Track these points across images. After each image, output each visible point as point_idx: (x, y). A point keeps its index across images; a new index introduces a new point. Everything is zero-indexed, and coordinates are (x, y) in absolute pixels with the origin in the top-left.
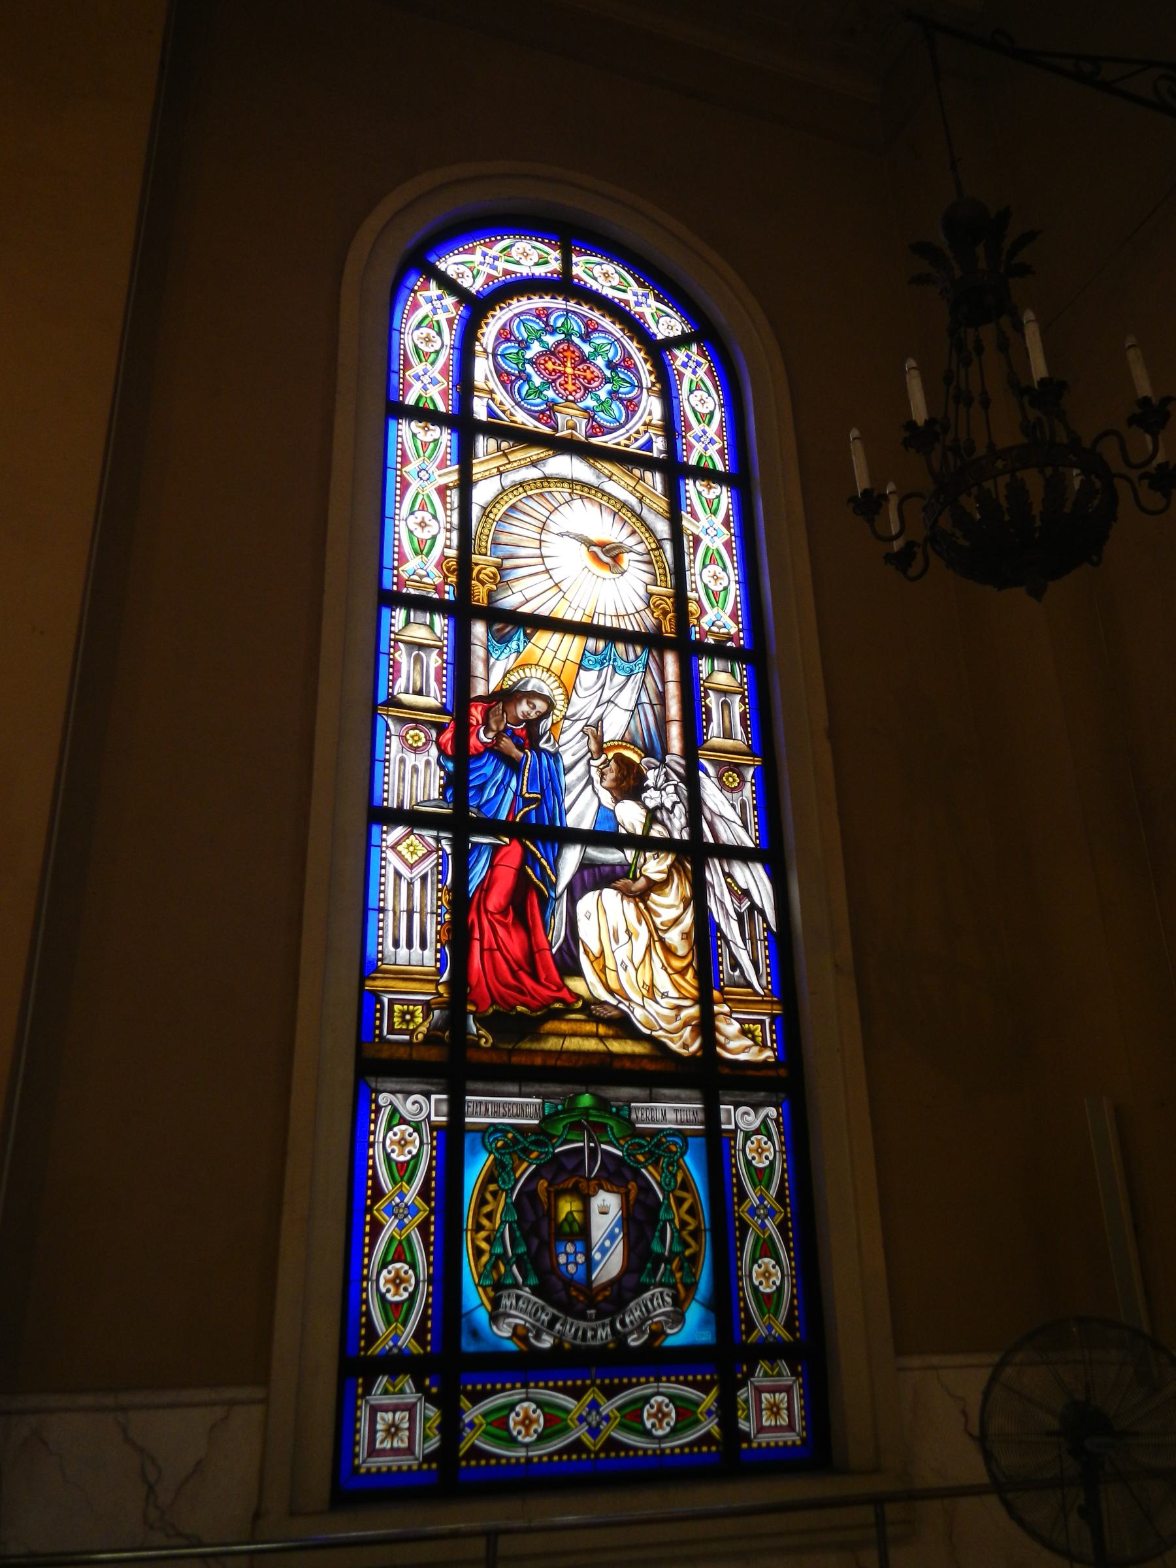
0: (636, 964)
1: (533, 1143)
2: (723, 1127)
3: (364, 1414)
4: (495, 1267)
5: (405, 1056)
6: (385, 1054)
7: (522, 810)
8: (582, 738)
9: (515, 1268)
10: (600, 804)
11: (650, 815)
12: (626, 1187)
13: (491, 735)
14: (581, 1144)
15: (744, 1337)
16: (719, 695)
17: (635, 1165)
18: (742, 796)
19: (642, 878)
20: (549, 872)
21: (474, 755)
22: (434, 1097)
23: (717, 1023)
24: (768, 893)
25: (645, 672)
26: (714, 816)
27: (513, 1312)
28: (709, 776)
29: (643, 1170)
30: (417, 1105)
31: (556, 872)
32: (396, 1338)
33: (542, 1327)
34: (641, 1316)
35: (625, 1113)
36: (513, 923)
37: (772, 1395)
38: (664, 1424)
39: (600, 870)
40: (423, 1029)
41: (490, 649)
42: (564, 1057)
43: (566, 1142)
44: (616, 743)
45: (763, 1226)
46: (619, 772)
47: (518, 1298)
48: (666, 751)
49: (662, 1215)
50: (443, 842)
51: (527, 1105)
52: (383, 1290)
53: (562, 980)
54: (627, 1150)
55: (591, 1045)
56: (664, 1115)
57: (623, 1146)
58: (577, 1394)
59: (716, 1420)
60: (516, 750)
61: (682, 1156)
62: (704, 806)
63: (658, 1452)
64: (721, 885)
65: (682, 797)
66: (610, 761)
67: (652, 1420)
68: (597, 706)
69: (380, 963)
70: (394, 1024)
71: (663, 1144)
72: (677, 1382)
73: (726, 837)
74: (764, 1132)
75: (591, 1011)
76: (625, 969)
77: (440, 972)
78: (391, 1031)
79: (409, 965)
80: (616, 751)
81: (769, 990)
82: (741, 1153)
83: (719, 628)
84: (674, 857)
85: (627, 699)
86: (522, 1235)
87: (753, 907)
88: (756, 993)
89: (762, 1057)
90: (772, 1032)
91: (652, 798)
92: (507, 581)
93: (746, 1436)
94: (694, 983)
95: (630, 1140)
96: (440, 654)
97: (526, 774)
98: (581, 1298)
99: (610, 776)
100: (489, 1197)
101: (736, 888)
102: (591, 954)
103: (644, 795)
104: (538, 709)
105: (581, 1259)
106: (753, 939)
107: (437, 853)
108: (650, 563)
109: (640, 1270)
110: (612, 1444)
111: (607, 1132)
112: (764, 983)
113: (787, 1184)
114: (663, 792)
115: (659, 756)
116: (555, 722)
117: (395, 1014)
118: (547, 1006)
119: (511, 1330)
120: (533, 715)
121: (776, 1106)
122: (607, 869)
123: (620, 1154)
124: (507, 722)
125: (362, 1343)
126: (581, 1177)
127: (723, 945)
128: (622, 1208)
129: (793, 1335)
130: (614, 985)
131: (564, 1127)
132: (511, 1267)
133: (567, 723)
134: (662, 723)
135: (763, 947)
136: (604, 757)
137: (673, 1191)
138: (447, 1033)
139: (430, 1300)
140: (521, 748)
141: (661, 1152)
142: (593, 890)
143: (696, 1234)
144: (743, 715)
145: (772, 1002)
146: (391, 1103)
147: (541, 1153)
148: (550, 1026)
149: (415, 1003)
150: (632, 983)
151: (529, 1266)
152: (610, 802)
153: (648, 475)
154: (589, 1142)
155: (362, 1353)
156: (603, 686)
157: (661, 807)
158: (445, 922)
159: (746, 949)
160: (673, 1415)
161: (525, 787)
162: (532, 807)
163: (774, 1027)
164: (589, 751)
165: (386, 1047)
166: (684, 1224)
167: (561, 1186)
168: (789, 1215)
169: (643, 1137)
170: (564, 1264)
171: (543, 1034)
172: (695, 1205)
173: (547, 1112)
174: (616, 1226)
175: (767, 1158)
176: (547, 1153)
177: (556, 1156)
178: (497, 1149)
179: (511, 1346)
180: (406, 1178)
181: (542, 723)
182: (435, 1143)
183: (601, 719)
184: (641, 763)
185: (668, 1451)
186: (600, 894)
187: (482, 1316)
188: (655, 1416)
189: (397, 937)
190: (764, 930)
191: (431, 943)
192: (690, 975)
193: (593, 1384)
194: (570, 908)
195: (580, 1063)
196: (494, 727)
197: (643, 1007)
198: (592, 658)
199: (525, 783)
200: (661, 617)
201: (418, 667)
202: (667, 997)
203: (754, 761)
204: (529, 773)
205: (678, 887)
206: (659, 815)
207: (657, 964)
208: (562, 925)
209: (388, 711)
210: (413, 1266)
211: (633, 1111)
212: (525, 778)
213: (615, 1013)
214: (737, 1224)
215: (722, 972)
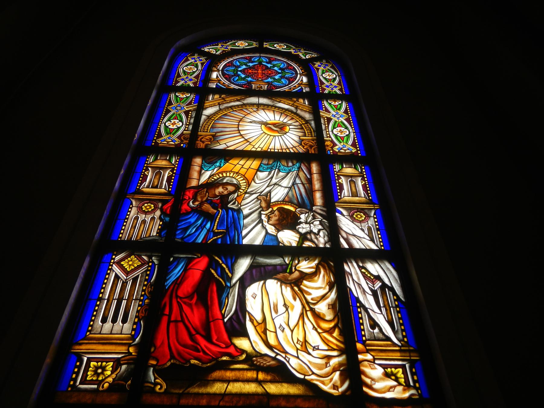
0: (292, 324)
6: (74, 400)
7: (212, 238)
8: (257, 201)
10: (267, 233)
11: (302, 237)
13: (197, 203)
16: (347, 178)
18: (368, 224)
19: (297, 273)
20: (227, 271)
21: (183, 213)
23: (362, 368)
24: (394, 277)
25: (299, 171)
26: (348, 235)
28: (344, 216)
31: (232, 271)
36: (196, 303)
39: (265, 269)
40: (110, 380)
41: (203, 167)
42: (226, 399)
44: (279, 203)
46: (281, 216)
48: (313, 204)
50: (153, 258)
53: (231, 340)
55: (251, 388)
60: (212, 210)
62: (341, 230)
64: (357, 274)
65: (325, 227)
66: (275, 211)
68: (268, 186)
73: (357, 245)
76: (283, 331)
77: (133, 338)
79: (111, 334)
80: (279, 206)
83: (345, 150)
84: (320, 259)
85: (287, 182)
87: (384, 286)
88: (395, 345)
89: (406, 395)
90: (413, 374)
91: (303, 228)
92: (217, 141)
96: (172, 171)
97: (217, 220)
99: (274, 219)
101: (369, 275)
102: (255, 321)
103: (297, 227)
104: (229, 190)
106: (387, 308)
107: (148, 264)
108: (302, 128)
112: (400, 336)
114: (311, 225)
115: (309, 207)
116: (239, 195)
118: (216, 359)
120: (226, 192)
122: (270, 268)
124: (208, 197)
127: (363, 312)
130: (272, 341)
133: (247, 195)
134: (310, 192)
135: (396, 311)
136: (270, 209)
140: (214, 207)
142: (259, 280)
144: (364, 187)
145: (409, 351)
148: (217, 374)
149: (107, 360)
150: (289, 341)
152: (274, 231)
153: (301, 101)
156: (272, 178)
157: (311, 232)
158: (145, 305)
159: (382, 313)
161: (215, 227)
162: (219, 236)
163: (414, 370)
164: (261, 207)
171: (211, 380)
181: (231, 196)
183: (270, 192)
184: (296, 211)
186: (265, 283)
190: (395, 300)
191: (131, 318)
192: (336, 334)
194: (241, 292)
195: (241, 403)
196: (199, 199)
197: (298, 357)
198: (266, 167)
199: (216, 224)
200: (309, 148)
201: (158, 177)
202: (318, 349)
203: (374, 206)
204: (219, 220)
205: (324, 276)
206: (309, 236)
207: (309, 326)
208: (233, 303)
209: (134, 196)
212: (216, 222)
213: (273, 362)
215: (364, 330)
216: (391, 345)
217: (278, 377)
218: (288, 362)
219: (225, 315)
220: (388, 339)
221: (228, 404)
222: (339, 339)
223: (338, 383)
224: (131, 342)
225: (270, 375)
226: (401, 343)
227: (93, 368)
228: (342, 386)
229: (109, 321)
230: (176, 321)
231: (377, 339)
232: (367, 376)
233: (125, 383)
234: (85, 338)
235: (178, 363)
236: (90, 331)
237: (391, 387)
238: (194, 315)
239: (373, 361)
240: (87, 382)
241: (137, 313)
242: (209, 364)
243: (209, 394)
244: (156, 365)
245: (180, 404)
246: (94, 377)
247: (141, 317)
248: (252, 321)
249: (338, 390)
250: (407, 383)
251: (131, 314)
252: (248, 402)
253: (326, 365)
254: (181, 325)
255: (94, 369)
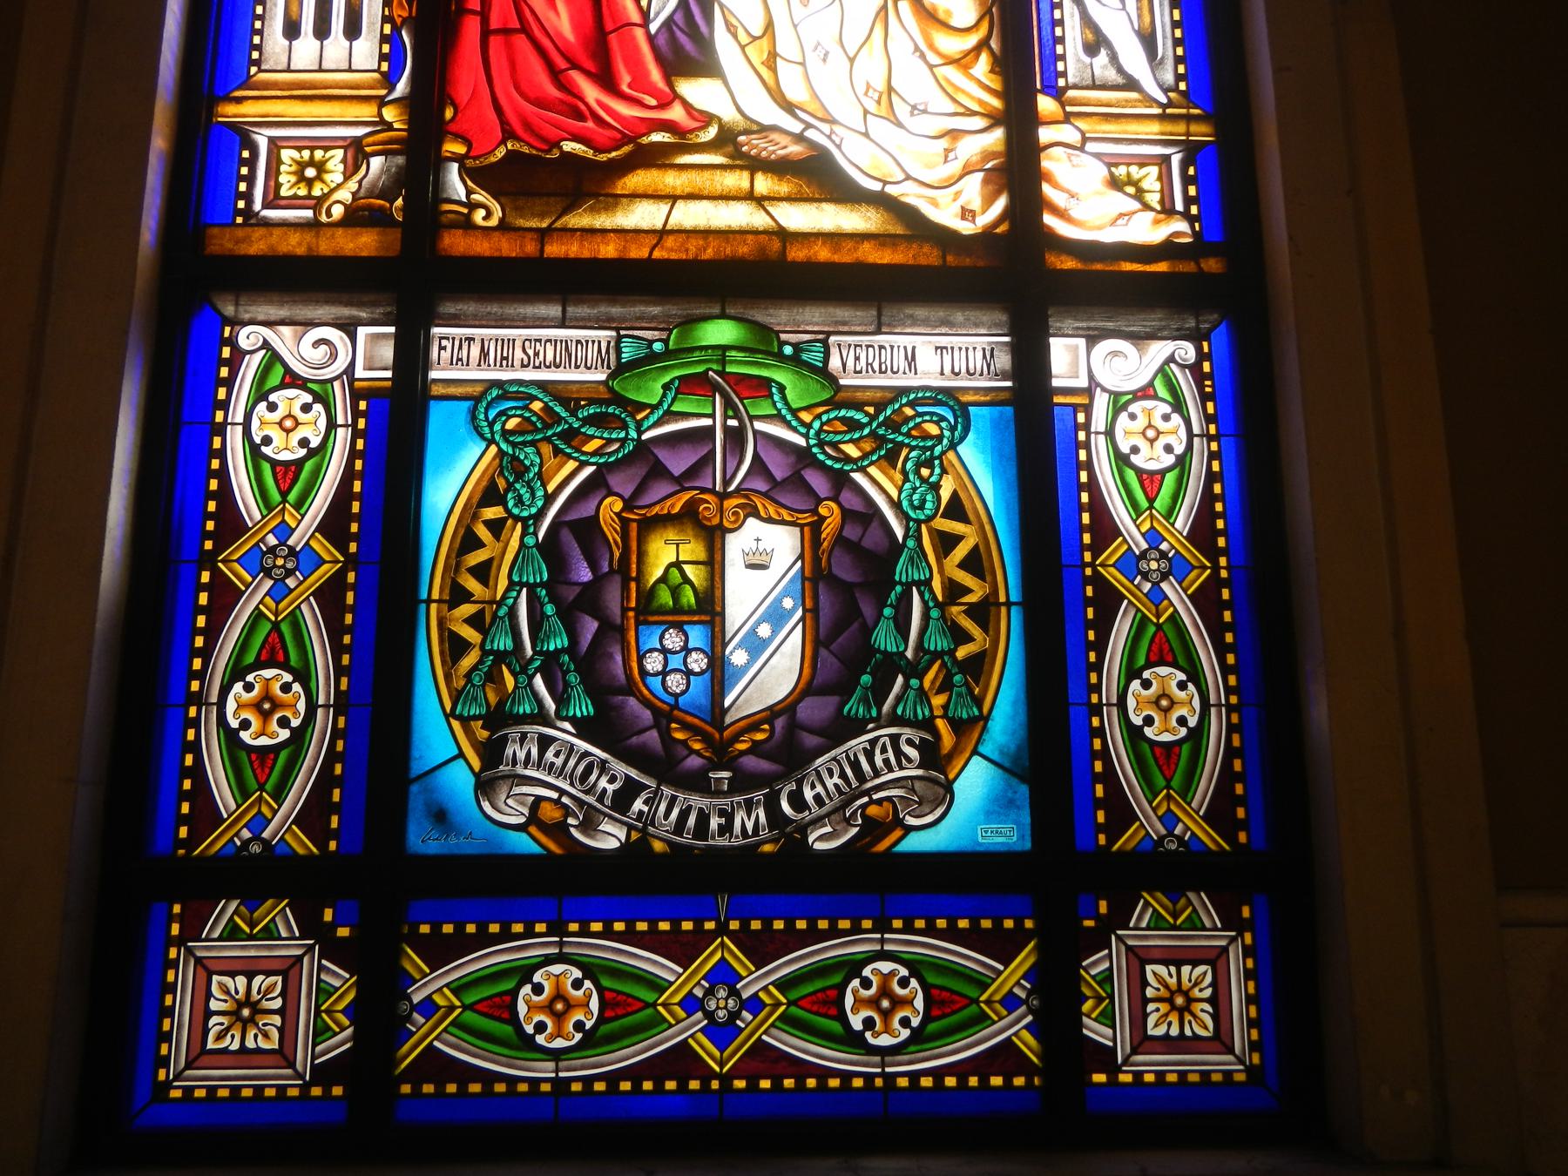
1: (589, 421)
2: (1056, 383)
3: (183, 977)
4: (493, 677)
5: (301, 251)
6: (258, 244)
9: (539, 682)
12: (815, 512)
14: (708, 422)
15: (1102, 839)
17: (837, 466)
22: (362, 332)
23: (1046, 164)
27: (528, 772)
29: (858, 477)
30: (324, 348)
32: (260, 822)
33: (599, 806)
34: (846, 789)
35: (814, 356)
37: (1173, 969)
38: (896, 1024)
40: (345, 195)
42: (670, 242)
43: (670, 415)
45: (1157, 597)
47: (545, 742)
49: (903, 570)
51: (578, 342)
52: (234, 724)
54: (818, 433)
56: (911, 360)
57: (809, 426)
58: (682, 950)
59: (1030, 1018)
61: (953, 446)
63: (879, 1082)
67: (866, 1013)
69: (254, 70)
70: (278, 186)
71: (907, 419)
72: (930, 931)
74: (1162, 392)
75: (738, 146)
77: (390, 80)
78: (273, 200)
79: (320, 70)
81: (1181, 93)
82: (1102, 438)
86: (559, 613)
88: (1151, 101)
90: (1186, 181)
93: (1104, 1057)
94: (995, 83)
95: (826, 412)
98: (697, 746)
100: (483, 532)
105: (698, 662)
109: (843, 688)
110: (763, 1058)
111: (771, 395)
112: (1169, 78)
113: (1219, 507)
117: (283, 168)
119: (526, 811)
121: (1195, 337)
123: (802, 442)
125: (183, 832)
126: (703, 490)
128: (801, 557)
129: (1231, 838)
131: (666, 387)
132: (531, 678)
137: (930, 519)
138: (399, 202)
139: (340, 746)
141: (900, 438)
143: (983, 613)
146: (266, 345)
147: (610, 441)
148: (638, 179)
149: (327, 145)
151: (573, 678)
154: (726, 417)
155: (181, 852)
159: (1124, 8)
160: (919, 1003)
163: (1191, 171)
165: (260, 231)
166: (955, 591)
167: (656, 509)
168: (1224, 574)
169: (858, 406)
170: (656, 674)
172: (982, 548)
173: (625, 357)
174: (785, 594)
175: (1168, 449)
176: (623, 441)
177: (643, 448)
178: (506, 433)
179: (524, 844)
180: (292, 497)
182: (362, 423)
185: (903, 1082)
187: (460, 781)
188: (873, 1003)
189: (294, 16)
191: (371, 24)
193: (722, 930)
195: (709, 254)
197: (866, 135)
202: (925, 112)
207: (900, 44)
210: (303, 675)
211: (834, 352)
213: (795, 149)
214: (1089, 591)
215: (1063, 57)
216: (1136, 101)
217: (809, 188)
218: (839, 147)
219: (652, 15)
220: (1131, 84)
221: (674, 256)
222: (988, 83)
223: (976, 203)
224: (383, 92)
225: (789, 181)
226: (1168, 97)
227: (290, 166)
228: (984, 212)
229: (306, 34)
230: (506, 31)
231: (1098, 83)
232: (1056, 186)
233: (388, 205)
234: (247, 83)
235: (527, 151)
236: (258, 63)
237: (1121, 215)
238: (558, 14)
239: (1079, 145)
240: (283, 202)
241: (386, 9)
242: (614, 154)
243: (620, 232)
244: (466, 156)
245: (545, 256)
246: (299, 188)
247: (401, 19)
248: (732, 30)
249: (973, 221)
250: (1168, 205)
251: (369, 11)
252: (728, 251)
253: (946, 157)
254: (521, 41)
255: (294, 168)
